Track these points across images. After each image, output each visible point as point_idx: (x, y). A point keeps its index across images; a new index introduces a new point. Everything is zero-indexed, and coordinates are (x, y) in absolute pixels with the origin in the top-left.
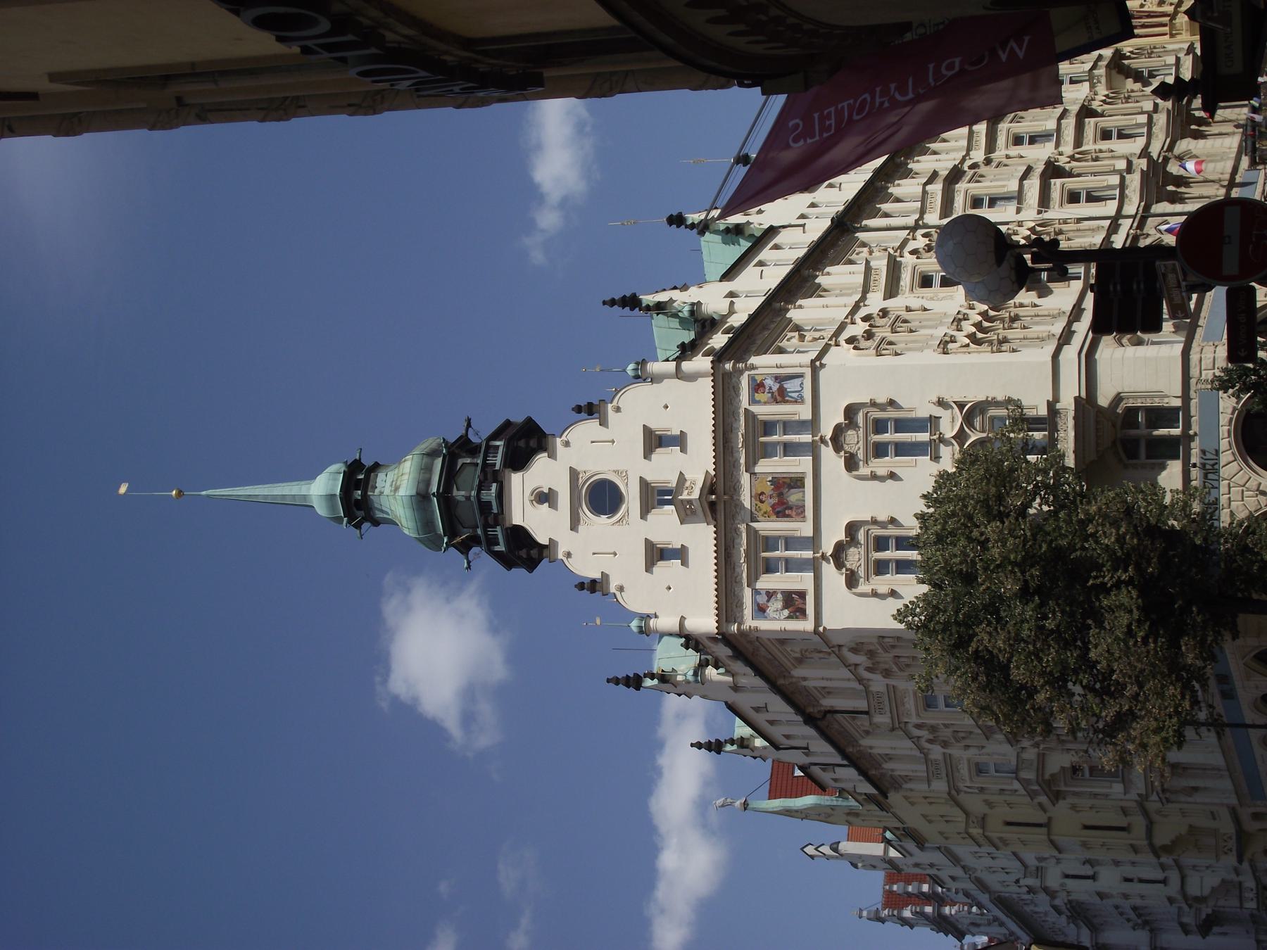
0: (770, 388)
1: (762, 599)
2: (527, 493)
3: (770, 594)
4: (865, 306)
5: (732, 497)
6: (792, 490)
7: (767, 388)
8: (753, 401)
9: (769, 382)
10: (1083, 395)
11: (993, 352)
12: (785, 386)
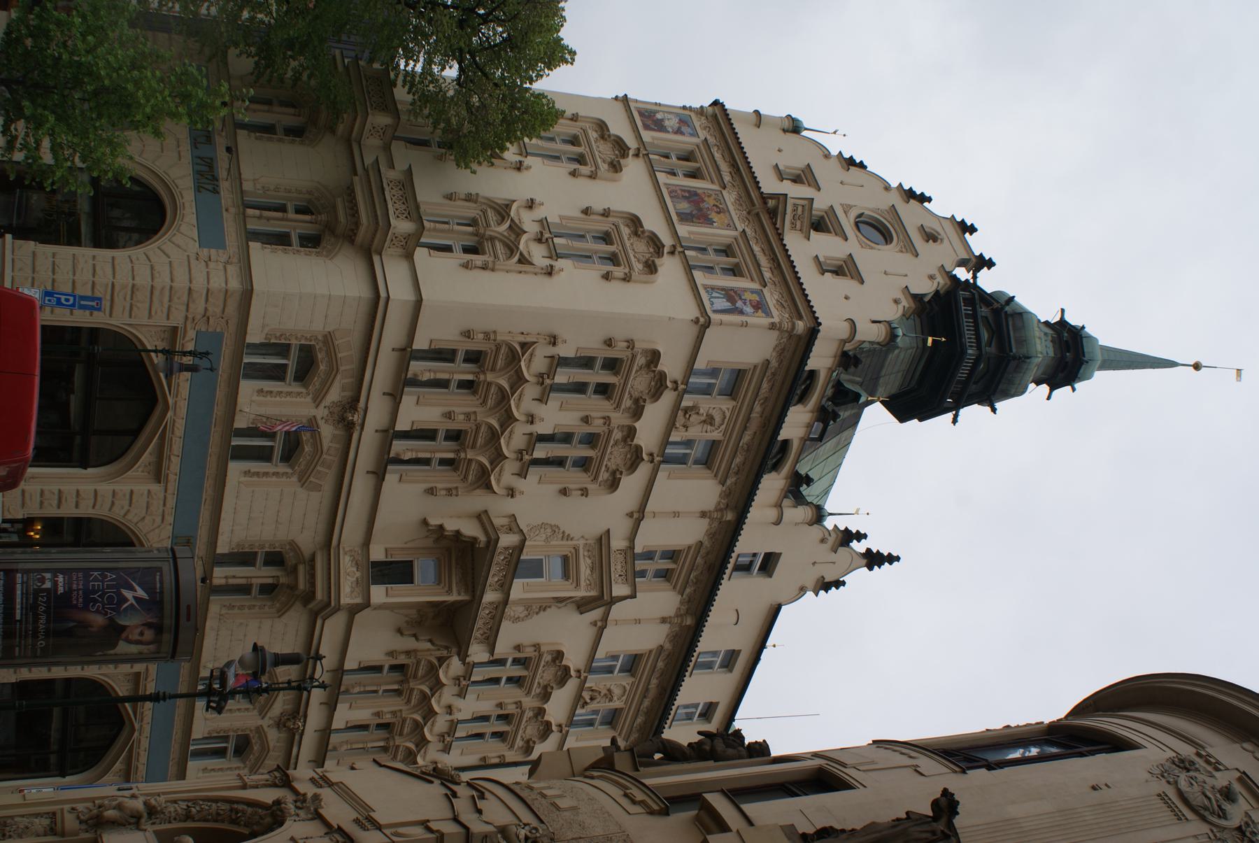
0: (745, 304)
1: (684, 129)
2: (946, 241)
3: (678, 131)
4: (630, 515)
5: (749, 213)
6: (689, 212)
7: (748, 303)
8: (760, 293)
9: (749, 309)
10: (376, 259)
11: (495, 332)
12: (729, 304)
